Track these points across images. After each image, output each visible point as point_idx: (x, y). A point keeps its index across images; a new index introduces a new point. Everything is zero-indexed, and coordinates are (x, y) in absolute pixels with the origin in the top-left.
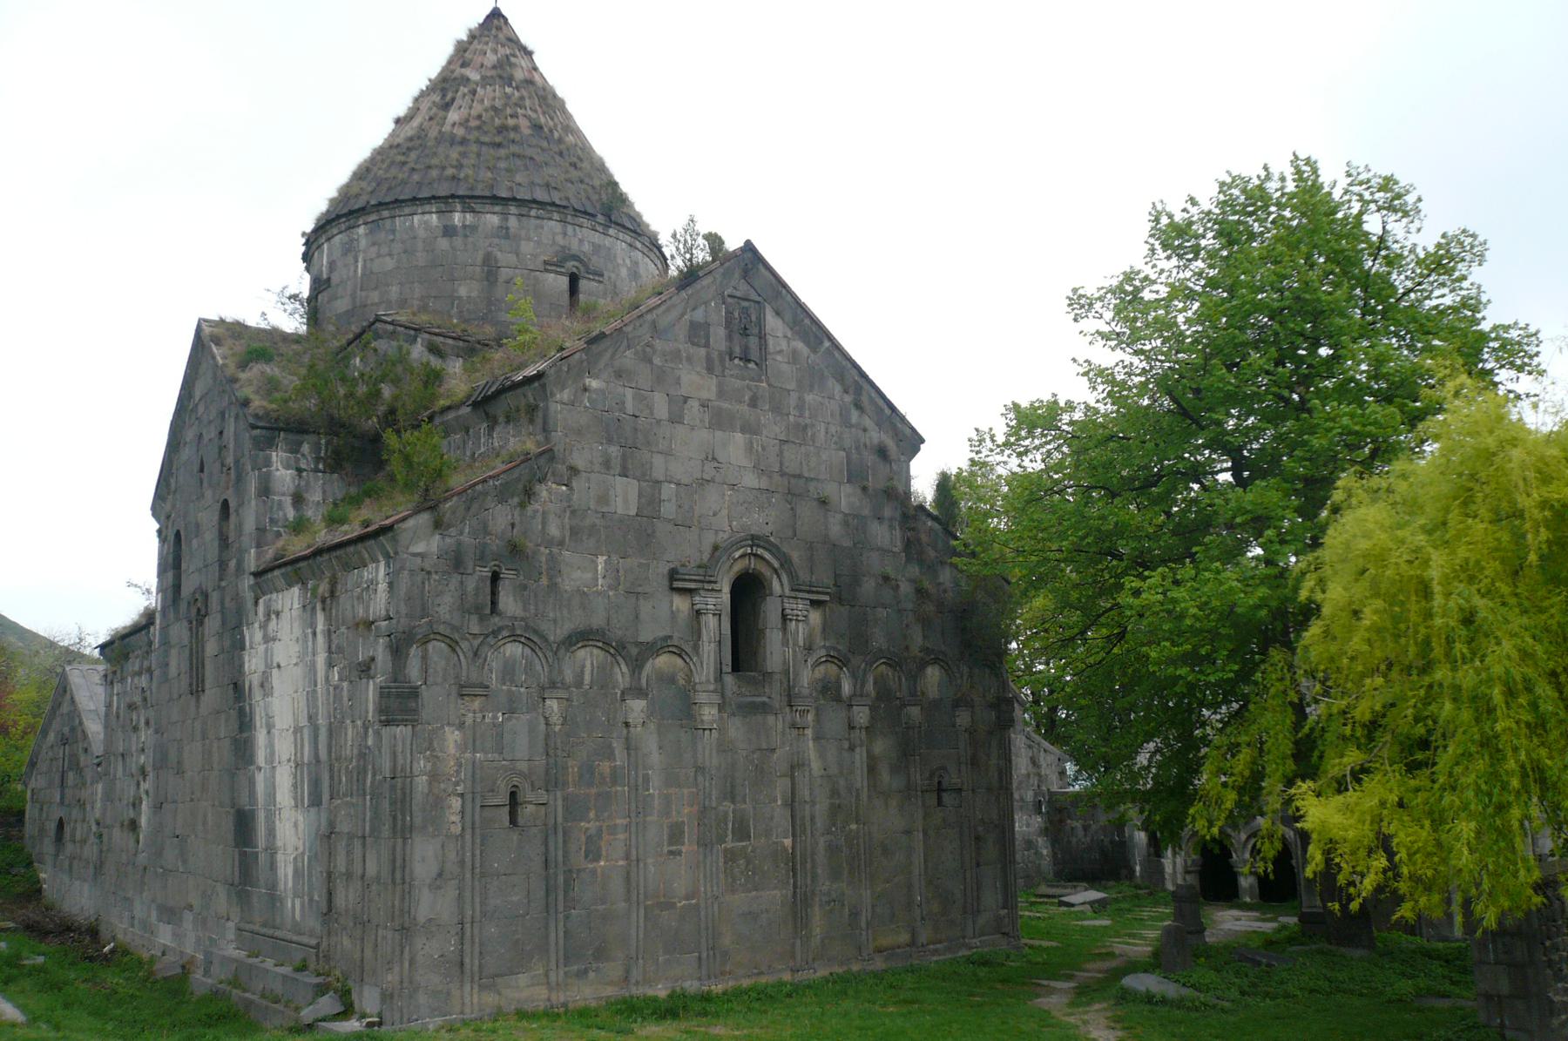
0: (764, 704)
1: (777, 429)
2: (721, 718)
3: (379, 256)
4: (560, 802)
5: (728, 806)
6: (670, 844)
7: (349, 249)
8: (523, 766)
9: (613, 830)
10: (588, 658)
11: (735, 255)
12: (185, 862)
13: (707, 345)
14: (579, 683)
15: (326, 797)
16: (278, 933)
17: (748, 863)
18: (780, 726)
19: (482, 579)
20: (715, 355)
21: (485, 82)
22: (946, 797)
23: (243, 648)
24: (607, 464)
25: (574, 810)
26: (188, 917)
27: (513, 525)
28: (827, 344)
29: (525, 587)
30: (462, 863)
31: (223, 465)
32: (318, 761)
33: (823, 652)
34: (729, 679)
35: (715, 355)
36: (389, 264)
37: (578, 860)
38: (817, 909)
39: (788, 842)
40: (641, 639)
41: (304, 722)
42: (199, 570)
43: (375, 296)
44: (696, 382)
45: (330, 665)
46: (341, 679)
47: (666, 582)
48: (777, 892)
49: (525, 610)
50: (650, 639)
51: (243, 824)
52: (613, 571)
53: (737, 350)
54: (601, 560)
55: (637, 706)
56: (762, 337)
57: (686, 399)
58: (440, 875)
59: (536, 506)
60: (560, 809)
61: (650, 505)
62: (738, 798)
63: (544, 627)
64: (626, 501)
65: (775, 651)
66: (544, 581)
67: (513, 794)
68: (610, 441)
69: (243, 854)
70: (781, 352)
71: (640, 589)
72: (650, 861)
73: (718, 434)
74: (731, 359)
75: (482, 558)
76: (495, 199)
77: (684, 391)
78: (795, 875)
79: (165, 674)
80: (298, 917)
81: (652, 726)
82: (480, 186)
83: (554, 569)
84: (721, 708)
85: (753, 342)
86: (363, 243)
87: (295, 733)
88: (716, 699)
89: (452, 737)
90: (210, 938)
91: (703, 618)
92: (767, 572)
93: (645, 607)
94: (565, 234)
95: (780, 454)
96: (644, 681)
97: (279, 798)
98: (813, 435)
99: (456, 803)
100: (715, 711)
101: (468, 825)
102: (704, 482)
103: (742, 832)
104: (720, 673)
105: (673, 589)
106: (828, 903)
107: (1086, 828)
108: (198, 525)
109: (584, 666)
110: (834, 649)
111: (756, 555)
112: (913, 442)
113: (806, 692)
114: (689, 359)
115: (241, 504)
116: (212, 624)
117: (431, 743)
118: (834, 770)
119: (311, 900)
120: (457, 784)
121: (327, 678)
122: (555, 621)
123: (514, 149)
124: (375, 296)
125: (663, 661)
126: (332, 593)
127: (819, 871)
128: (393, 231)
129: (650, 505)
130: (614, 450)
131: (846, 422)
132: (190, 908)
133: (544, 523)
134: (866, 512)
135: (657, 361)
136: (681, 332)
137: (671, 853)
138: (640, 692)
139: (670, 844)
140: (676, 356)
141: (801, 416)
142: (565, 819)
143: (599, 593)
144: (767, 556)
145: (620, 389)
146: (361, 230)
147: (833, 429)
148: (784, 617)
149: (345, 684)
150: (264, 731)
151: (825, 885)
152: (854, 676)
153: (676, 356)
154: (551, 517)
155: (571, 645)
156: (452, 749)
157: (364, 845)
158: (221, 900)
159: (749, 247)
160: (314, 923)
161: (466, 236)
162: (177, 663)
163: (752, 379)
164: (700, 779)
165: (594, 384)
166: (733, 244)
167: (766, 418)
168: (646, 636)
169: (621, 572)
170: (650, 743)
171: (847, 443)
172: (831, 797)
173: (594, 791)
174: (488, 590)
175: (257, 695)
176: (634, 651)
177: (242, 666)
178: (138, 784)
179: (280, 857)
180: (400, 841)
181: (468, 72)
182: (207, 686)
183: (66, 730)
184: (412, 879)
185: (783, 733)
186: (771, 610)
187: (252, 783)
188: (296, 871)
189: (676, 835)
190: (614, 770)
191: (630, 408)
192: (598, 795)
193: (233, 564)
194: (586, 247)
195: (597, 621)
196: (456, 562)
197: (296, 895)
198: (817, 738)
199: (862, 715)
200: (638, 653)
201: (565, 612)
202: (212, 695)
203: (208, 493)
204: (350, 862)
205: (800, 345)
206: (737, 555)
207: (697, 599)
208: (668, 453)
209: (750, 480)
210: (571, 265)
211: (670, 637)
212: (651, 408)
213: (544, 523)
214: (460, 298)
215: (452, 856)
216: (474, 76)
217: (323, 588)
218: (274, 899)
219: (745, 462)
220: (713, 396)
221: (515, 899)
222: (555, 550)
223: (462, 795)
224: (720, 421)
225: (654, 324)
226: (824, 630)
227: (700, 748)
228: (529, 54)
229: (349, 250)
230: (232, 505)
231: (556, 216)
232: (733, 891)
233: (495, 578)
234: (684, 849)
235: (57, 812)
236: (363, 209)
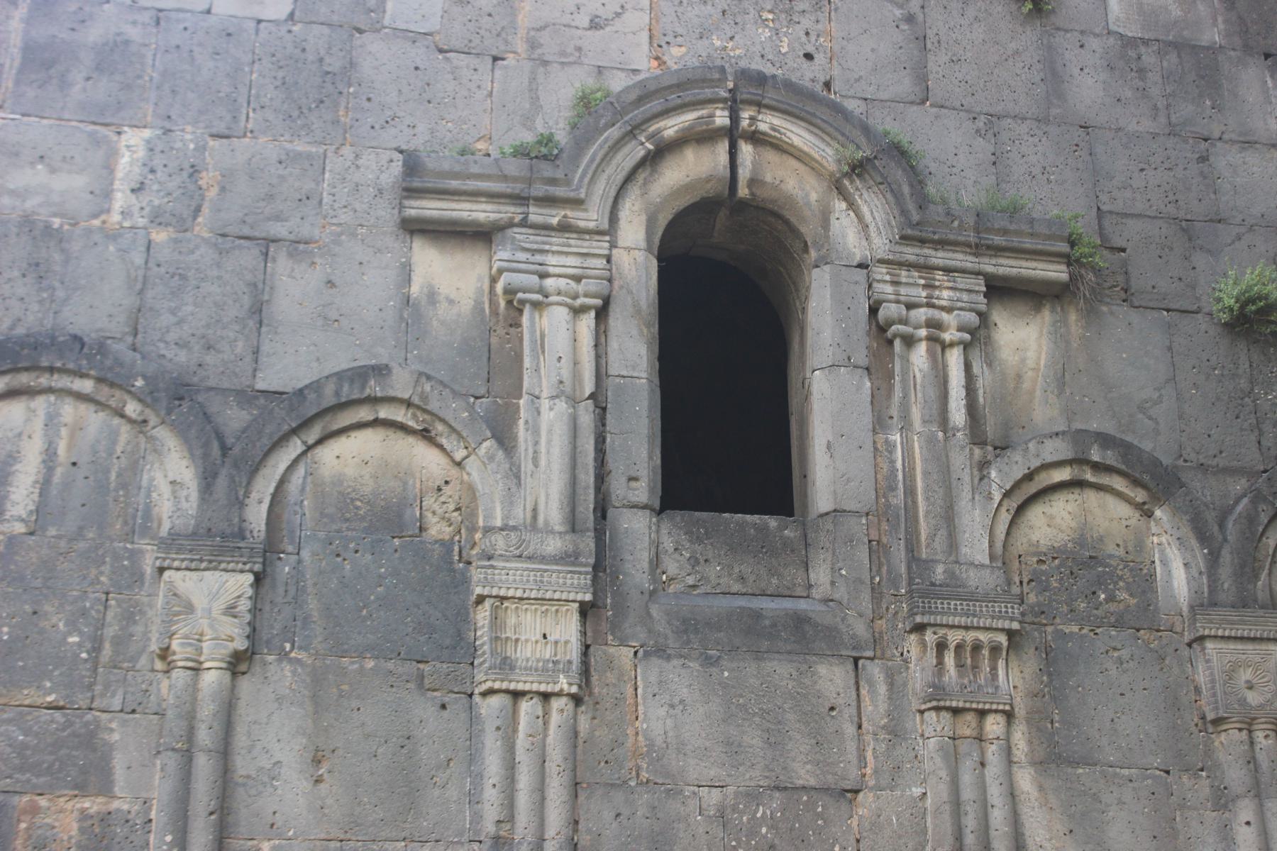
0: (799, 622)
18: (876, 707)
33: (1056, 449)
47: (386, 214)
50: (303, 377)
71: (279, 230)
88: (577, 586)
93: (294, 287)
100: (568, 629)
104: (597, 514)
105: (416, 228)
110: (1105, 440)
111: (756, 138)
113: (982, 579)
125: (352, 457)
134: (1213, 35)
138: (214, 542)
143: (112, 235)
144: (798, 135)
152: (1204, 532)
168: (291, 365)
169: (205, 179)
185: (895, 732)
195: (95, 310)
198: (1056, 757)
200: (243, 428)
206: (671, 127)
211: (381, 371)
226: (1061, 383)
227: (493, 765)
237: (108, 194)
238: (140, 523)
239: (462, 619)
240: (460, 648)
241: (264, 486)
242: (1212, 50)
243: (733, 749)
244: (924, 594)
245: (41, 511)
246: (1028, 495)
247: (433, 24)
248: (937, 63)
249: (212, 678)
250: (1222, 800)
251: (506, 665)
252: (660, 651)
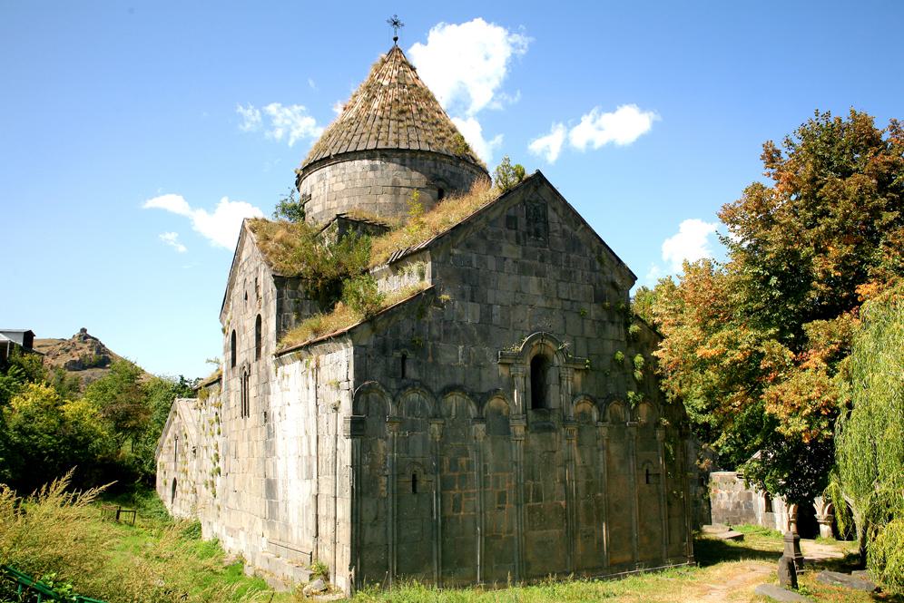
1: (555, 274)
2: (526, 434)
3: (336, 182)
4: (439, 480)
5: (530, 482)
6: (499, 503)
7: (321, 178)
8: (419, 460)
9: (468, 495)
10: (454, 400)
11: (529, 179)
12: (240, 505)
13: (516, 229)
14: (449, 415)
17: (541, 514)
18: (558, 440)
19: (398, 358)
20: (521, 234)
21: (391, 86)
22: (651, 478)
23: (269, 393)
24: (463, 296)
25: (446, 485)
26: (242, 534)
27: (413, 330)
28: (582, 226)
29: (419, 363)
30: (387, 512)
31: (258, 296)
32: (310, 455)
34: (530, 412)
35: (521, 234)
36: (342, 186)
37: (449, 512)
38: (579, 540)
39: (563, 503)
40: (482, 391)
41: (303, 434)
42: (246, 351)
43: (335, 204)
44: (510, 250)
48: (557, 531)
49: (420, 375)
51: (271, 487)
52: (467, 353)
53: (533, 230)
54: (461, 347)
55: (482, 427)
56: (546, 223)
57: (505, 259)
58: (376, 519)
59: (426, 319)
60: (439, 484)
61: (486, 316)
62: (536, 478)
63: (430, 384)
64: (473, 315)
65: (554, 398)
66: (430, 359)
67: (414, 476)
68: (464, 282)
69: (271, 503)
70: (556, 231)
72: (488, 512)
73: (523, 277)
74: (530, 235)
75: (397, 348)
76: (398, 150)
77: (504, 254)
78: (567, 522)
79: (228, 405)
80: (300, 537)
81: (489, 439)
82: (390, 143)
83: (435, 353)
84: (526, 428)
85: (540, 226)
86: (329, 175)
89: (382, 444)
90: (254, 546)
91: (515, 379)
92: (549, 352)
93: (484, 373)
94: (436, 167)
95: (557, 287)
96: (484, 414)
98: (575, 277)
99: (384, 480)
100: (523, 429)
101: (390, 492)
102: (515, 305)
103: (538, 497)
104: (525, 412)
106: (586, 537)
107: (729, 495)
108: (244, 328)
109: (451, 407)
112: (633, 278)
113: (572, 419)
114: (507, 237)
115: (267, 317)
116: (253, 380)
117: (371, 449)
118: (588, 463)
119: (307, 529)
120: (385, 469)
122: (436, 381)
123: (408, 122)
124: (335, 204)
126: (317, 366)
127: (581, 519)
128: (344, 169)
129: (486, 316)
130: (467, 288)
131: (593, 269)
132: (243, 529)
133: (430, 328)
134: (605, 319)
135: (489, 238)
136: (502, 223)
137: (499, 508)
138: (480, 419)
139: (499, 503)
140: (499, 235)
141: (569, 266)
142: (442, 489)
144: (551, 344)
145: (470, 255)
146: (327, 169)
147: (586, 273)
148: (560, 378)
151: (583, 527)
152: (599, 409)
153: (499, 235)
154: (434, 324)
155: (445, 394)
156: (382, 451)
158: (259, 526)
159: (539, 174)
160: (309, 543)
161: (382, 170)
162: (235, 399)
163: (541, 247)
164: (514, 467)
165: (456, 252)
166: (530, 172)
167: (549, 267)
168: (484, 389)
170: (489, 449)
171: (594, 281)
172: (587, 478)
173: (457, 474)
174: (400, 365)
175: (277, 418)
176: (479, 397)
178: (215, 464)
179: (290, 506)
181: (381, 80)
183: (177, 432)
184: (361, 520)
186: (552, 375)
187: (274, 465)
189: (502, 498)
190: (468, 462)
191: (475, 266)
192: (459, 476)
193: (263, 349)
194: (447, 174)
195: (459, 381)
196: (383, 349)
198: (579, 445)
199: (603, 431)
201: (441, 376)
202: (254, 417)
203: (250, 311)
204: (328, 510)
205: (566, 227)
207: (512, 369)
208: (496, 289)
209: (541, 303)
210: (441, 184)
212: (486, 264)
213: (430, 328)
214: (380, 203)
215: (382, 509)
216: (386, 83)
217: (313, 364)
218: (287, 526)
219: (539, 293)
220: (520, 257)
221: (416, 532)
222: (435, 342)
223: (387, 476)
224: (524, 270)
225: (487, 218)
227: (514, 451)
228: (413, 69)
229: (321, 180)
230: (263, 317)
231: (430, 157)
232: (534, 530)
233: (404, 358)
234: (506, 506)
235: (172, 476)
236: (329, 157)
237: (458, 358)
238: (469, 417)
239: (509, 428)
240: (509, 433)
241: (484, 410)
242: (605, 322)
243: (542, 446)
244: (565, 421)
245: (456, 416)
246: (579, 403)
247: (498, 323)
248: (568, 326)
249: (482, 440)
250: (599, 450)
251: (516, 436)
252: (532, 432)
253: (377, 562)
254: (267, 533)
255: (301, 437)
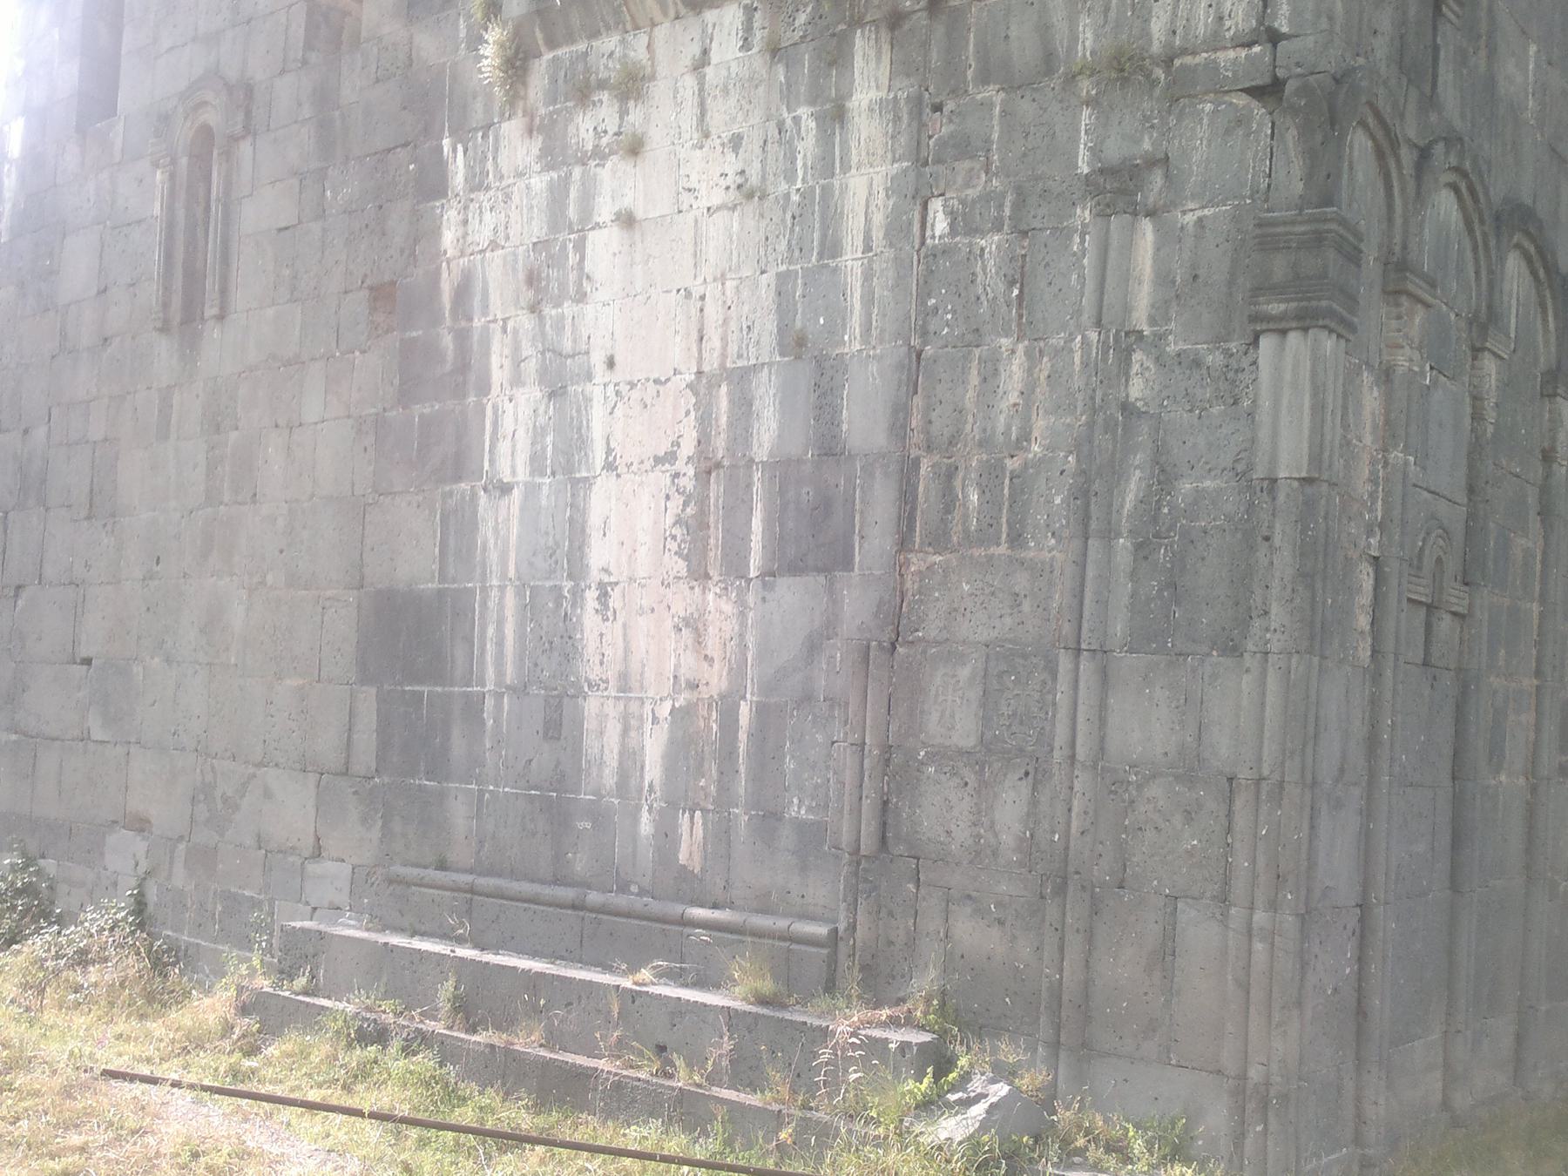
15: (873, 543)
16: (594, 897)
23: (433, 186)
32: (830, 448)
45: (915, 193)
46: (962, 223)
87: (703, 385)
97: (600, 554)
119: (769, 819)
121: (897, 230)
132: (140, 825)
149: (991, 243)
150: (531, 395)
157: (1104, 676)
177: (424, 234)
180: (1316, 660)
182: (240, 299)
188: (683, 747)
197: (675, 802)
253: (1335, 990)
254: (354, 842)
255: (740, 379)
